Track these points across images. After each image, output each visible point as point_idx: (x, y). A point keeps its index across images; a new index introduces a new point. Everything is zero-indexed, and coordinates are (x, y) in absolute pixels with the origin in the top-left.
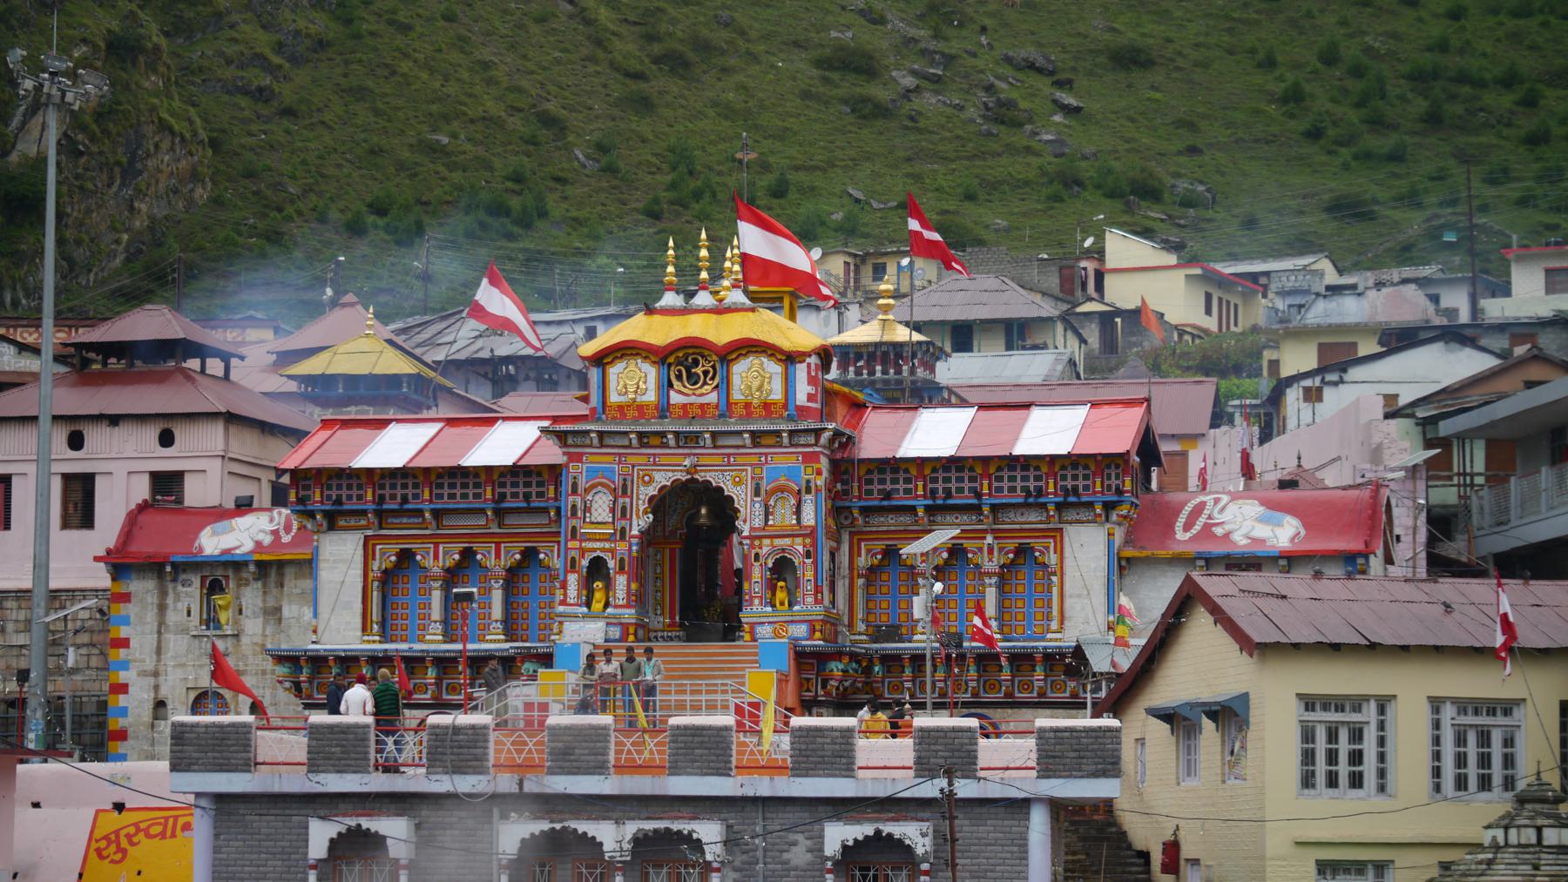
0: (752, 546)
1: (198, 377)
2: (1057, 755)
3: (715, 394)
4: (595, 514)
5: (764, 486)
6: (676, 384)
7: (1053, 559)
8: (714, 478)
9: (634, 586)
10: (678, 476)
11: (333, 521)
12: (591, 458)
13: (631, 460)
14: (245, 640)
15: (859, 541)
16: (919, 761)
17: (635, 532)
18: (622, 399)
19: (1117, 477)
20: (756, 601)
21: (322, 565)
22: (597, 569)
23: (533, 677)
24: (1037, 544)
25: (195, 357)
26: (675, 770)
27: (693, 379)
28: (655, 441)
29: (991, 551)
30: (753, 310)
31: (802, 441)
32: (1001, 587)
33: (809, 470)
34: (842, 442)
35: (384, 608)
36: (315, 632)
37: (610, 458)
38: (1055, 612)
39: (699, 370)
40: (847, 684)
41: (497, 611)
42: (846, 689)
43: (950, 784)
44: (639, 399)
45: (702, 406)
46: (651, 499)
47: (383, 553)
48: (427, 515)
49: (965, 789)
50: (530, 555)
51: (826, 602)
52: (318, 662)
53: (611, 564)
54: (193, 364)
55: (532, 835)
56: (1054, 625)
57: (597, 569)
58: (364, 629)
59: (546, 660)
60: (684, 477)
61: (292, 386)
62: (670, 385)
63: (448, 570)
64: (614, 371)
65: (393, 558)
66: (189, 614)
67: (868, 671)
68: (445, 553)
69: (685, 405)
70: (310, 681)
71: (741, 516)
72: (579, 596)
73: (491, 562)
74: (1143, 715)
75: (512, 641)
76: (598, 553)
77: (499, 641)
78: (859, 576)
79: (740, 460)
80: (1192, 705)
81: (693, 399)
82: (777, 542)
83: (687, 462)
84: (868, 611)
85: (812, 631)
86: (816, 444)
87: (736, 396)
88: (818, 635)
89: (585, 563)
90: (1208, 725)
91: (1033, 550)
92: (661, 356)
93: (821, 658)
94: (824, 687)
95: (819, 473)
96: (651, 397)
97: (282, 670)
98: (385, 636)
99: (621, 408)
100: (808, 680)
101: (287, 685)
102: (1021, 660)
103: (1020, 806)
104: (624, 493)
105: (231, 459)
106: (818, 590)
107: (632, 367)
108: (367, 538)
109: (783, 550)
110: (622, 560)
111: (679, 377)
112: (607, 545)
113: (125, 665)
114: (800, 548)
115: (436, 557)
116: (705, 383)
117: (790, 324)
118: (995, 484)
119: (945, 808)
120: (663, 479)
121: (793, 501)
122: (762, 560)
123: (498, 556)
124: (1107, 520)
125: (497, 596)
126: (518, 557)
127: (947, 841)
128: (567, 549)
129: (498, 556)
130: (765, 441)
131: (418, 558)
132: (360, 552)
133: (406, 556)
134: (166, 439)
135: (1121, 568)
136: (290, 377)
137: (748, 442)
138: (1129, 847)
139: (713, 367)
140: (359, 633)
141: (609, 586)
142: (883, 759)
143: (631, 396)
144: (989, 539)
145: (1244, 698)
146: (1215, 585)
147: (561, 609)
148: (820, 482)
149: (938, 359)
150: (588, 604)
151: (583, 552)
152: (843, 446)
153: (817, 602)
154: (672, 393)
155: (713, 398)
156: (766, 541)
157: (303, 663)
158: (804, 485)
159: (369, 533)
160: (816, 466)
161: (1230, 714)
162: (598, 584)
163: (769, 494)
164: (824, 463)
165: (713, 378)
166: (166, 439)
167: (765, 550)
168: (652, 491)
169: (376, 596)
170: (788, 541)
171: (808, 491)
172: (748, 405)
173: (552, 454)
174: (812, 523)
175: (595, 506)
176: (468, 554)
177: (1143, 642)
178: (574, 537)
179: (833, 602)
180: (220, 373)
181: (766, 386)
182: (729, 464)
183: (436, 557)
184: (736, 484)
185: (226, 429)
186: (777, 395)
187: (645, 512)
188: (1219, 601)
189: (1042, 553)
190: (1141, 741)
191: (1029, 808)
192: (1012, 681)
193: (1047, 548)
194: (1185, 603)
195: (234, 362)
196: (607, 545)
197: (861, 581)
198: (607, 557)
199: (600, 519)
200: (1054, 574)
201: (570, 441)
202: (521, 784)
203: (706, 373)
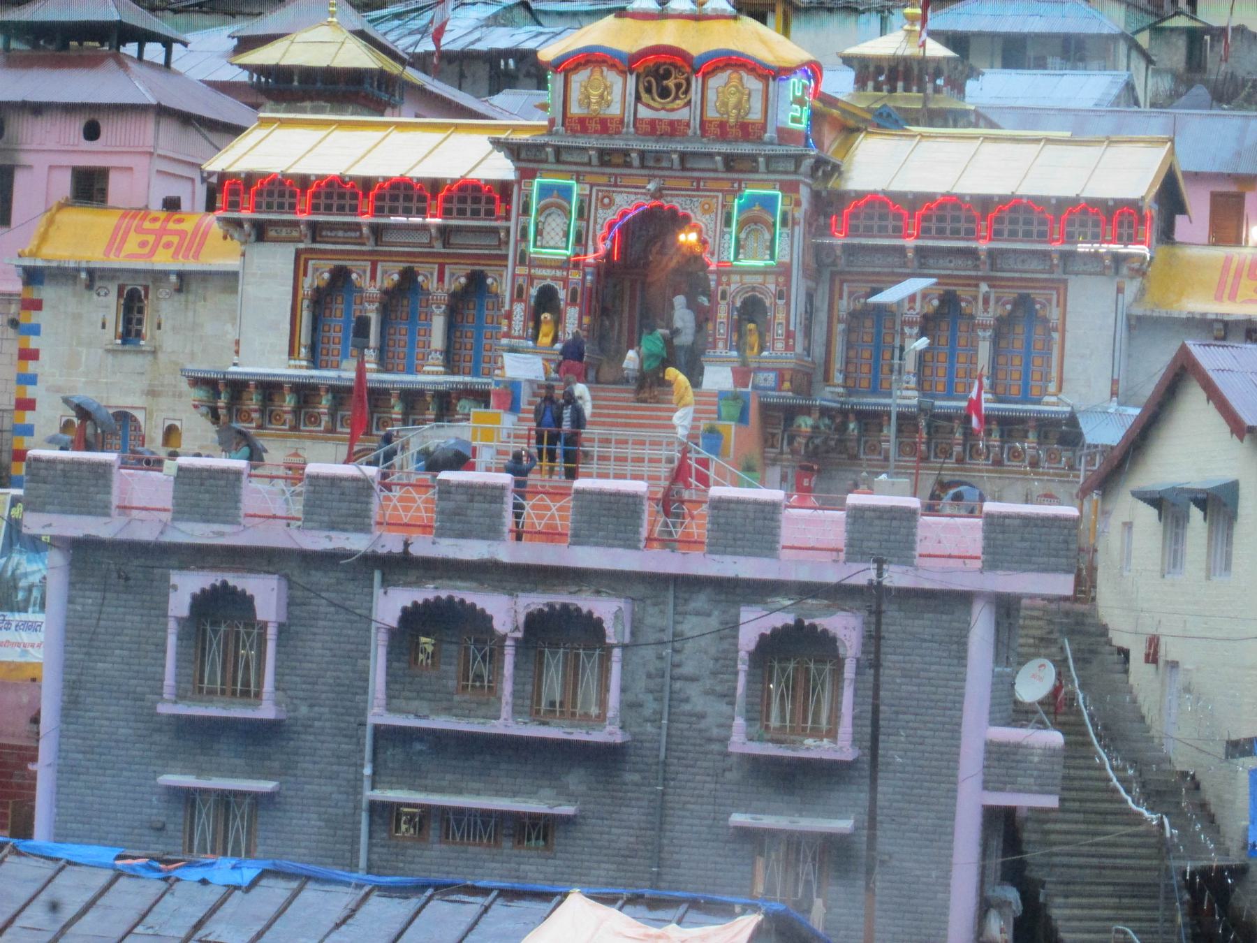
0: (719, 283)
1: (134, 67)
2: (1007, 542)
3: (686, 110)
6: (645, 97)
7: (1054, 314)
9: (586, 320)
11: (261, 232)
14: (160, 355)
15: (842, 282)
16: (851, 544)
17: (590, 259)
19: (1130, 227)
20: (721, 344)
22: (547, 300)
23: (467, 418)
24: (1038, 295)
25: (132, 41)
26: (578, 539)
27: (664, 93)
28: (617, 159)
29: (986, 301)
30: (735, 18)
32: (996, 340)
34: (826, 169)
35: (315, 329)
36: (237, 352)
38: (1054, 374)
39: (671, 83)
40: (817, 441)
41: (437, 338)
42: (816, 447)
43: (880, 575)
45: (672, 123)
47: (316, 269)
48: (365, 230)
49: (896, 577)
50: (477, 282)
51: (799, 349)
52: (237, 387)
53: (562, 294)
54: (131, 49)
55: (415, 603)
56: (1052, 387)
57: (547, 300)
58: (292, 352)
59: (481, 397)
60: (648, 202)
61: (243, 76)
63: (386, 292)
64: (579, 79)
65: (326, 276)
66: (104, 326)
67: (842, 428)
68: (384, 272)
69: (653, 123)
70: (229, 408)
72: (525, 327)
73: (433, 285)
74: (1130, 498)
75: (453, 373)
76: (549, 282)
77: (437, 373)
78: (840, 321)
79: (711, 185)
80: (1179, 491)
81: (662, 115)
82: (748, 279)
83: (651, 186)
84: (848, 361)
85: (781, 379)
86: (795, 172)
88: (787, 385)
89: (533, 292)
90: (1196, 514)
91: (1034, 302)
92: (627, 64)
93: (790, 413)
94: (790, 443)
95: (798, 203)
97: (199, 394)
98: (315, 360)
99: (582, 121)
100: (773, 435)
101: (204, 410)
102: (1009, 426)
103: (964, 599)
105: (159, 156)
106: (789, 335)
107: (597, 75)
109: (753, 289)
110: (574, 292)
111: (648, 90)
113: (32, 380)
114: (772, 287)
115: (373, 277)
116: (677, 97)
117: (781, 38)
118: (995, 226)
119: (873, 599)
122: (729, 299)
123: (441, 278)
124: (1117, 272)
125: (438, 324)
126: (463, 280)
127: (874, 639)
128: (514, 276)
129: (441, 278)
130: (738, 166)
131: (354, 276)
133: (340, 277)
134: (92, 132)
135: (1130, 327)
136: (244, 67)
137: (720, 166)
138: (1109, 643)
140: (286, 356)
141: (558, 320)
142: (812, 536)
144: (984, 288)
145: (1232, 489)
146: (1209, 357)
147: (505, 341)
148: (800, 213)
149: (968, 77)
150: (535, 338)
151: (531, 279)
152: (827, 176)
153: (788, 348)
154: (640, 107)
155: (683, 114)
156: (735, 278)
157: (221, 387)
159: (301, 246)
160: (794, 196)
161: (1219, 504)
162: (546, 316)
164: (804, 193)
166: (92, 132)
167: (733, 287)
168: (611, 215)
169: (305, 317)
170: (760, 279)
172: (722, 125)
173: (501, 168)
175: (547, 229)
176: (408, 276)
177: (1137, 411)
178: (522, 263)
179: (808, 350)
180: (161, 60)
182: (698, 189)
183: (373, 277)
184: (705, 212)
185: (158, 123)
186: (755, 116)
188: (1214, 376)
189: (1043, 306)
190: (1128, 526)
191: (971, 603)
192: (1002, 448)
193: (1049, 301)
194: (1183, 372)
195: (176, 48)
196: (559, 273)
197: (841, 327)
198: (558, 286)
199: (552, 243)
200: (1055, 330)
201: (523, 155)
202: (406, 544)
203: (678, 86)
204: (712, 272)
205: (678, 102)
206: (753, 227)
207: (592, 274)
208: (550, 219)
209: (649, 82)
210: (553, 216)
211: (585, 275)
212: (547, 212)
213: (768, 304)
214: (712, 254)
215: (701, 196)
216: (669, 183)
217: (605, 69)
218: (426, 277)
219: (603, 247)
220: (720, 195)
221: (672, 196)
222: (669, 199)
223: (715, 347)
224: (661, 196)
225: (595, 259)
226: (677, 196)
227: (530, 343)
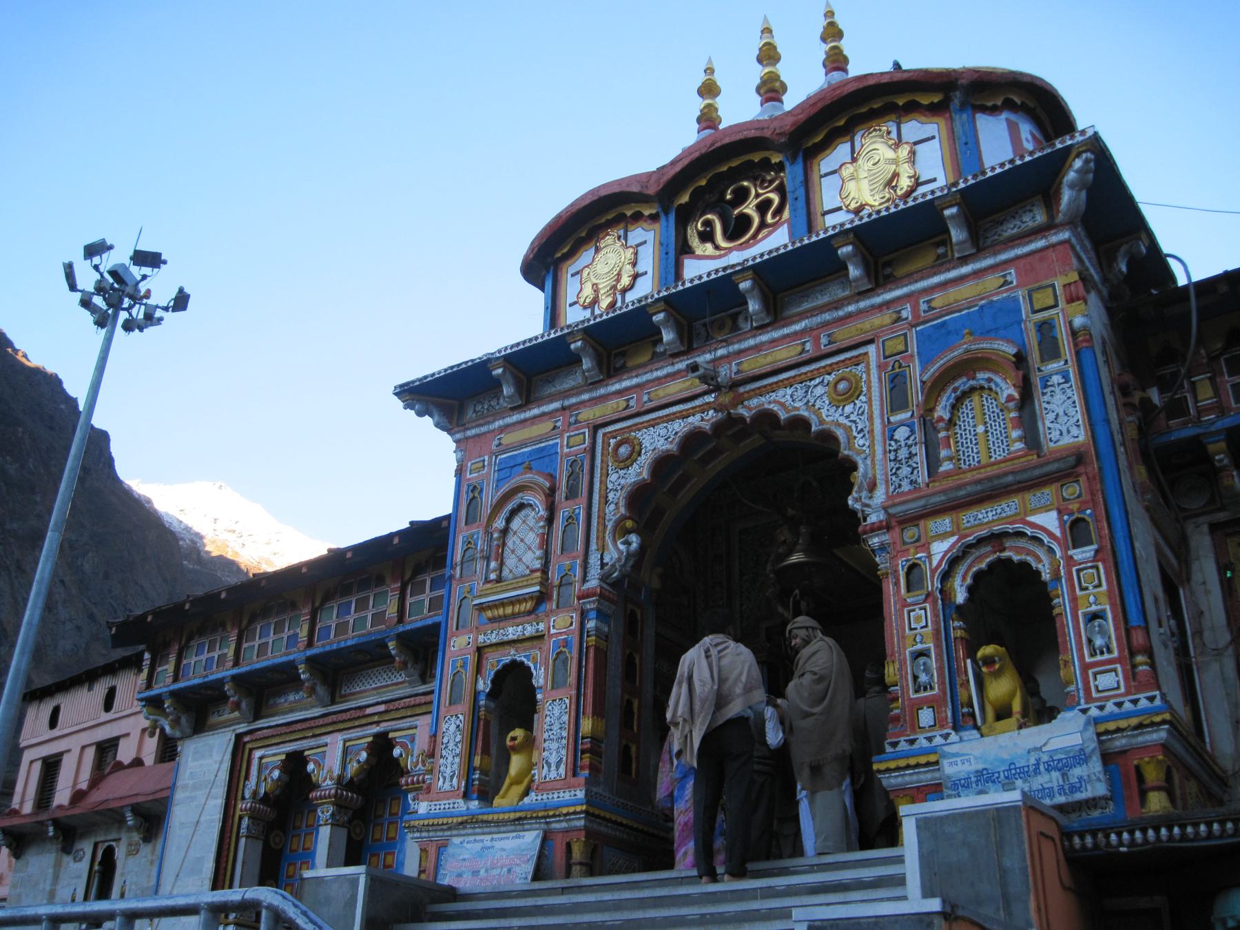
4: (510, 561)
5: (917, 375)
8: (786, 401)
9: (587, 725)
10: (695, 420)
12: (508, 439)
13: (587, 414)
20: (926, 716)
21: (179, 795)
22: (510, 700)
31: (1010, 230)
33: (1044, 298)
37: (546, 426)
39: (749, 209)
46: (638, 497)
60: (704, 420)
71: (859, 476)
89: (484, 685)
104: (572, 494)
108: (239, 737)
109: (996, 539)
111: (707, 237)
112: (530, 630)
114: (1049, 520)
120: (658, 440)
121: (1008, 389)
132: (226, 765)
139: (781, 190)
158: (1032, 339)
159: (242, 728)
163: (935, 388)
165: (779, 211)
168: (639, 471)
171: (1050, 350)
174: (1080, 435)
175: (510, 543)
187: (621, 530)
201: (470, 414)
203: (763, 207)
204: (875, 529)
205: (765, 231)
206: (962, 384)
207: (601, 615)
208: (516, 524)
209: (708, 223)
210: (523, 513)
211: (583, 615)
212: (509, 506)
213: (1046, 576)
214: (872, 487)
215: (829, 370)
216: (752, 365)
218: (404, 746)
219: (616, 551)
220: (871, 349)
221: (760, 392)
222: (754, 402)
223: (915, 726)
224: (739, 400)
225: (603, 579)
226: (773, 388)
227: (474, 804)
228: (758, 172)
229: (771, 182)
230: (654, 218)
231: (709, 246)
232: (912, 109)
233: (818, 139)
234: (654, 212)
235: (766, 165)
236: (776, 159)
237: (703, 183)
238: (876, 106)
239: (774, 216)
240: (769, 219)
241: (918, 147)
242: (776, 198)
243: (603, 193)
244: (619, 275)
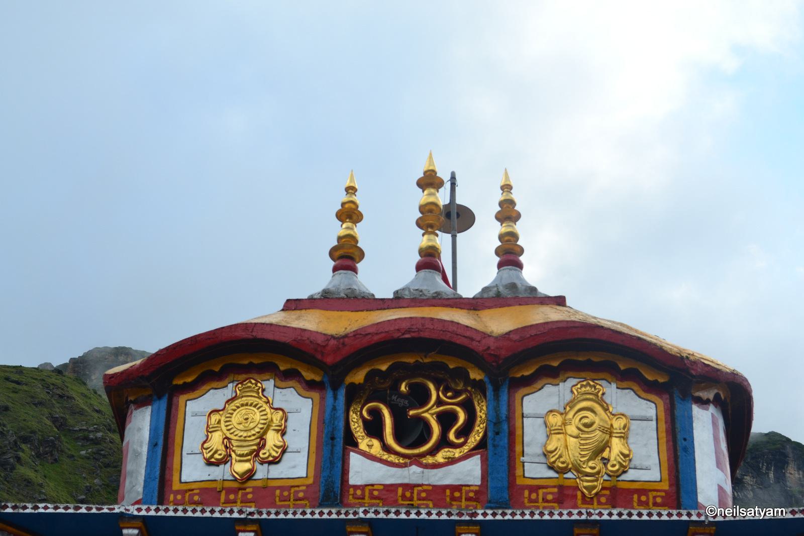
6: (364, 443)
18: (217, 473)
27: (411, 433)
44: (262, 472)
62: (351, 442)
69: (390, 489)
81: (413, 474)
87: (534, 470)
96: (296, 466)
111: (374, 428)
116: (444, 442)
143: (242, 467)
154: (355, 459)
155: (469, 472)
165: (465, 432)
181: (617, 445)
203: (447, 419)
209: (376, 414)
217: (269, 385)
228: (448, 380)
229: (457, 394)
230: (311, 386)
231: (376, 443)
232: (627, 378)
233: (527, 373)
234: (318, 378)
235: (462, 374)
236: (475, 375)
237: (384, 368)
238: (596, 359)
239: (458, 436)
240: (452, 436)
241: (634, 425)
242: (462, 417)
243: (259, 335)
244: (262, 438)
